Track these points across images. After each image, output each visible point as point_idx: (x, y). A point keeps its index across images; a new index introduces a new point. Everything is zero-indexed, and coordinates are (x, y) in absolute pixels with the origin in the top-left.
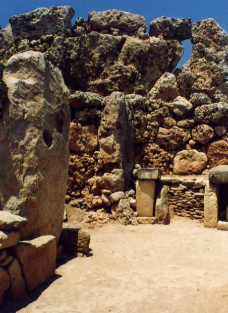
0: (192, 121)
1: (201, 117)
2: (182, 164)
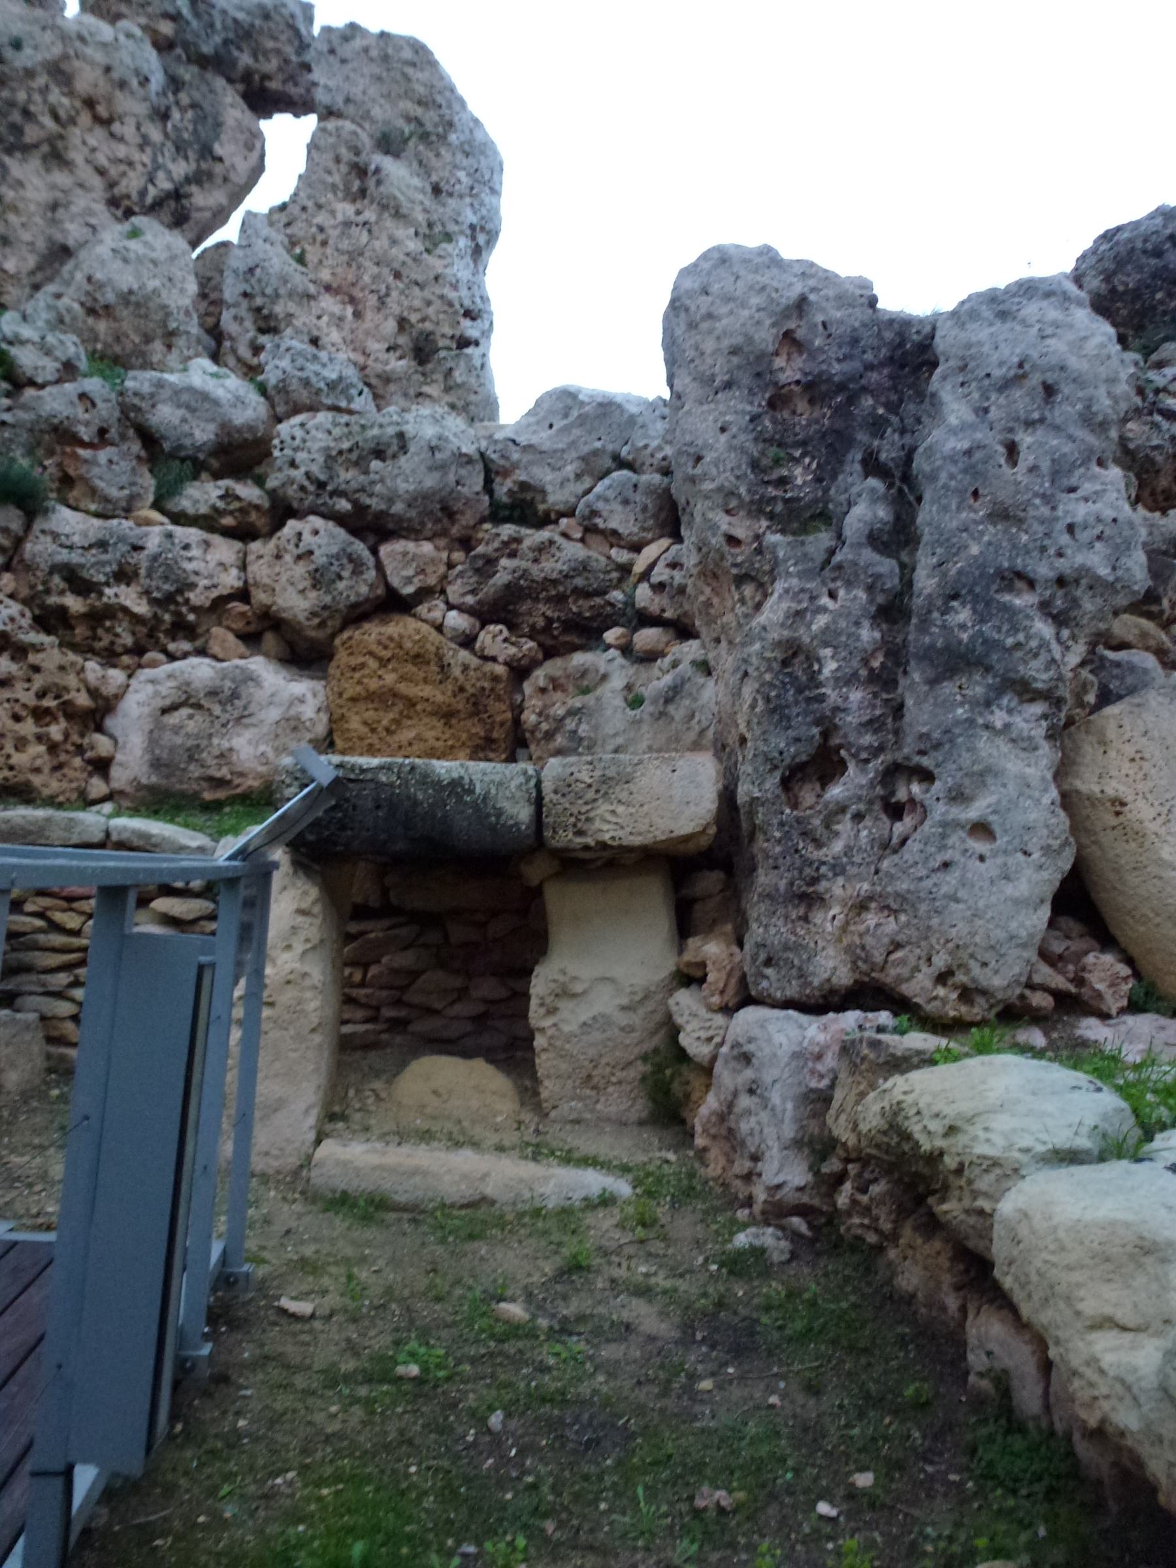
0: (248, 492)
1: (308, 475)
2: (168, 738)
